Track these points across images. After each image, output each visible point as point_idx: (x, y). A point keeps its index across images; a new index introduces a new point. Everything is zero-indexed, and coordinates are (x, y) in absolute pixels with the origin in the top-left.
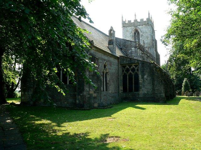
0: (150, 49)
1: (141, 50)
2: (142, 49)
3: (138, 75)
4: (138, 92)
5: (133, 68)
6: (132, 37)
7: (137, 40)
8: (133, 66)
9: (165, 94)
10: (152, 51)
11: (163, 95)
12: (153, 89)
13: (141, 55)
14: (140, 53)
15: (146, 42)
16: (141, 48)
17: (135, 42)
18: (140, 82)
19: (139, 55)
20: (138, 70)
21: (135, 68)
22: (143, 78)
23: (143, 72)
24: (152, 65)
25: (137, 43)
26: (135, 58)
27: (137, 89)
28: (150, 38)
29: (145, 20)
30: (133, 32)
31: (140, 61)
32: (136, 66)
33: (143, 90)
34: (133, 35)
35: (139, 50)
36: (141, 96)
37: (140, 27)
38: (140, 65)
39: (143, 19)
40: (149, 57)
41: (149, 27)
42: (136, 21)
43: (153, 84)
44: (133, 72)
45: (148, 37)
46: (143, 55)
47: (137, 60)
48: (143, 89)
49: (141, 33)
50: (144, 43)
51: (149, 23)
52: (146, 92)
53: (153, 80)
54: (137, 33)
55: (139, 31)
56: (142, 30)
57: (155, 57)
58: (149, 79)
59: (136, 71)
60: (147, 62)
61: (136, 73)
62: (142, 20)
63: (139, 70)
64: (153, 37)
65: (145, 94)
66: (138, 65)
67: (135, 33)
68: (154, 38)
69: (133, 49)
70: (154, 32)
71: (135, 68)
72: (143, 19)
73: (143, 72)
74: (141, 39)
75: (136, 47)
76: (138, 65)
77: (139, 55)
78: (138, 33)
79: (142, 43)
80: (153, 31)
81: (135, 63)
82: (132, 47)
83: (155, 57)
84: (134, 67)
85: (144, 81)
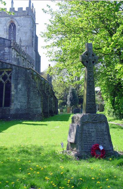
0: (28, 48)
1: (17, 51)
2: (18, 50)
3: (10, 84)
4: (9, 107)
5: (5, 75)
6: (6, 31)
7: (12, 38)
8: (5, 72)
9: (43, 110)
10: (30, 52)
11: (40, 110)
12: (28, 102)
13: (16, 56)
14: (14, 55)
15: (23, 38)
16: (17, 48)
17: (10, 40)
18: (13, 93)
19: (13, 57)
20: (10, 78)
21: (7, 75)
22: (16, 88)
23: (16, 80)
24: (28, 71)
25: (12, 41)
26: (8, 61)
27: (8, 103)
28: (29, 34)
29: (24, 9)
30: (8, 25)
31: (14, 65)
32: (8, 72)
33: (15, 104)
34: (8, 28)
35: (14, 50)
36: (12, 112)
37: (17, 18)
38: (14, 71)
39: (22, 8)
40: (26, 59)
41: (28, 19)
42: (12, 9)
43: (28, 96)
44: (4, 81)
45: (27, 33)
46: (19, 57)
47: (11, 65)
48: (15, 102)
49: (17, 27)
50: (21, 41)
51: (30, 13)
52: (19, 107)
53: (29, 90)
54: (12, 27)
55: (16, 23)
56: (19, 22)
57: (34, 59)
58: (23, 89)
59: (8, 79)
60: (23, 68)
61: (8, 81)
62: (20, 9)
63: (12, 78)
64: (33, 33)
65: (17, 110)
66: (11, 71)
67: (10, 27)
68: (34, 33)
69: (7, 49)
70: (36, 26)
71: (7, 75)
72: (22, 8)
73: (16, 80)
74: (17, 34)
75: (10, 47)
76: (11, 71)
77: (13, 57)
78: (15, 26)
79: (18, 41)
80: (34, 25)
81: (8, 69)
82: (4, 46)
83: (33, 60)
84: (6, 73)
85: (17, 93)
